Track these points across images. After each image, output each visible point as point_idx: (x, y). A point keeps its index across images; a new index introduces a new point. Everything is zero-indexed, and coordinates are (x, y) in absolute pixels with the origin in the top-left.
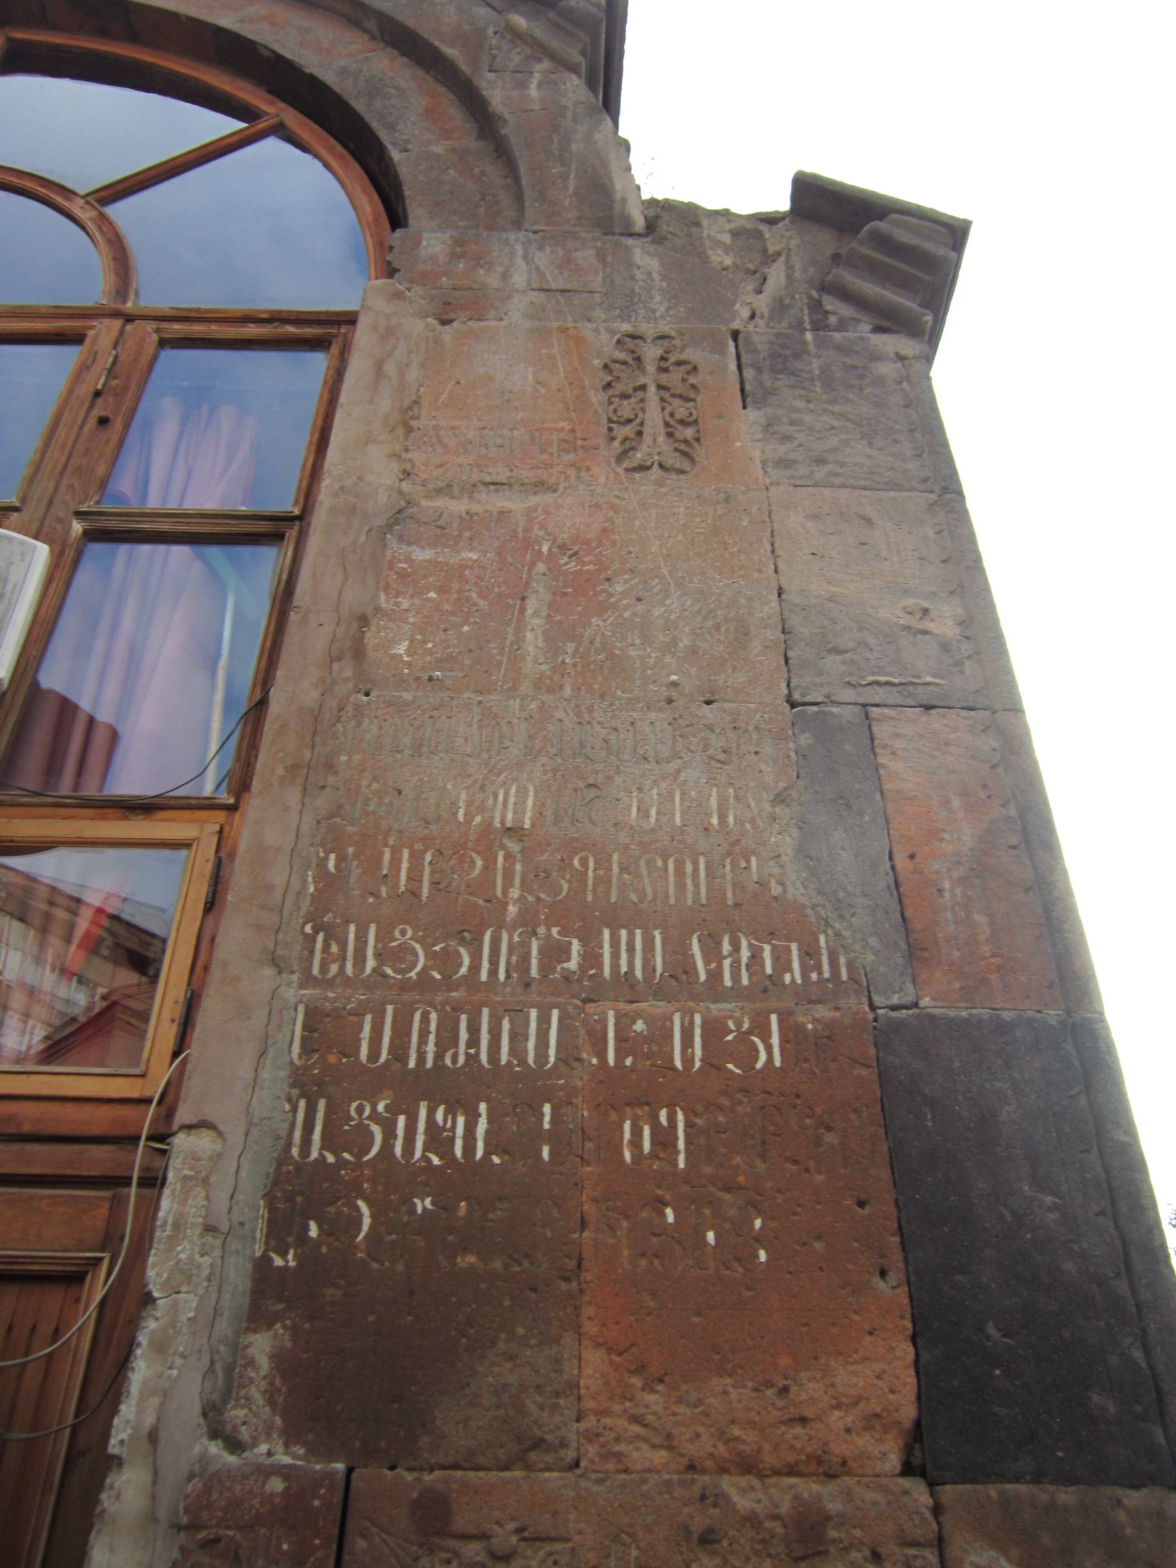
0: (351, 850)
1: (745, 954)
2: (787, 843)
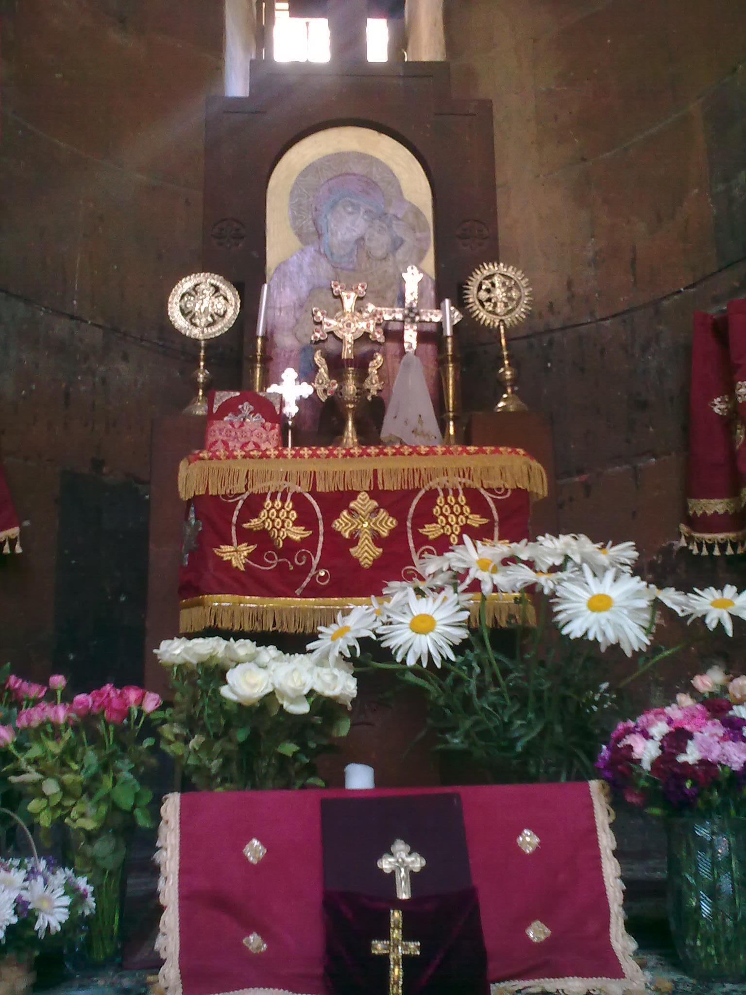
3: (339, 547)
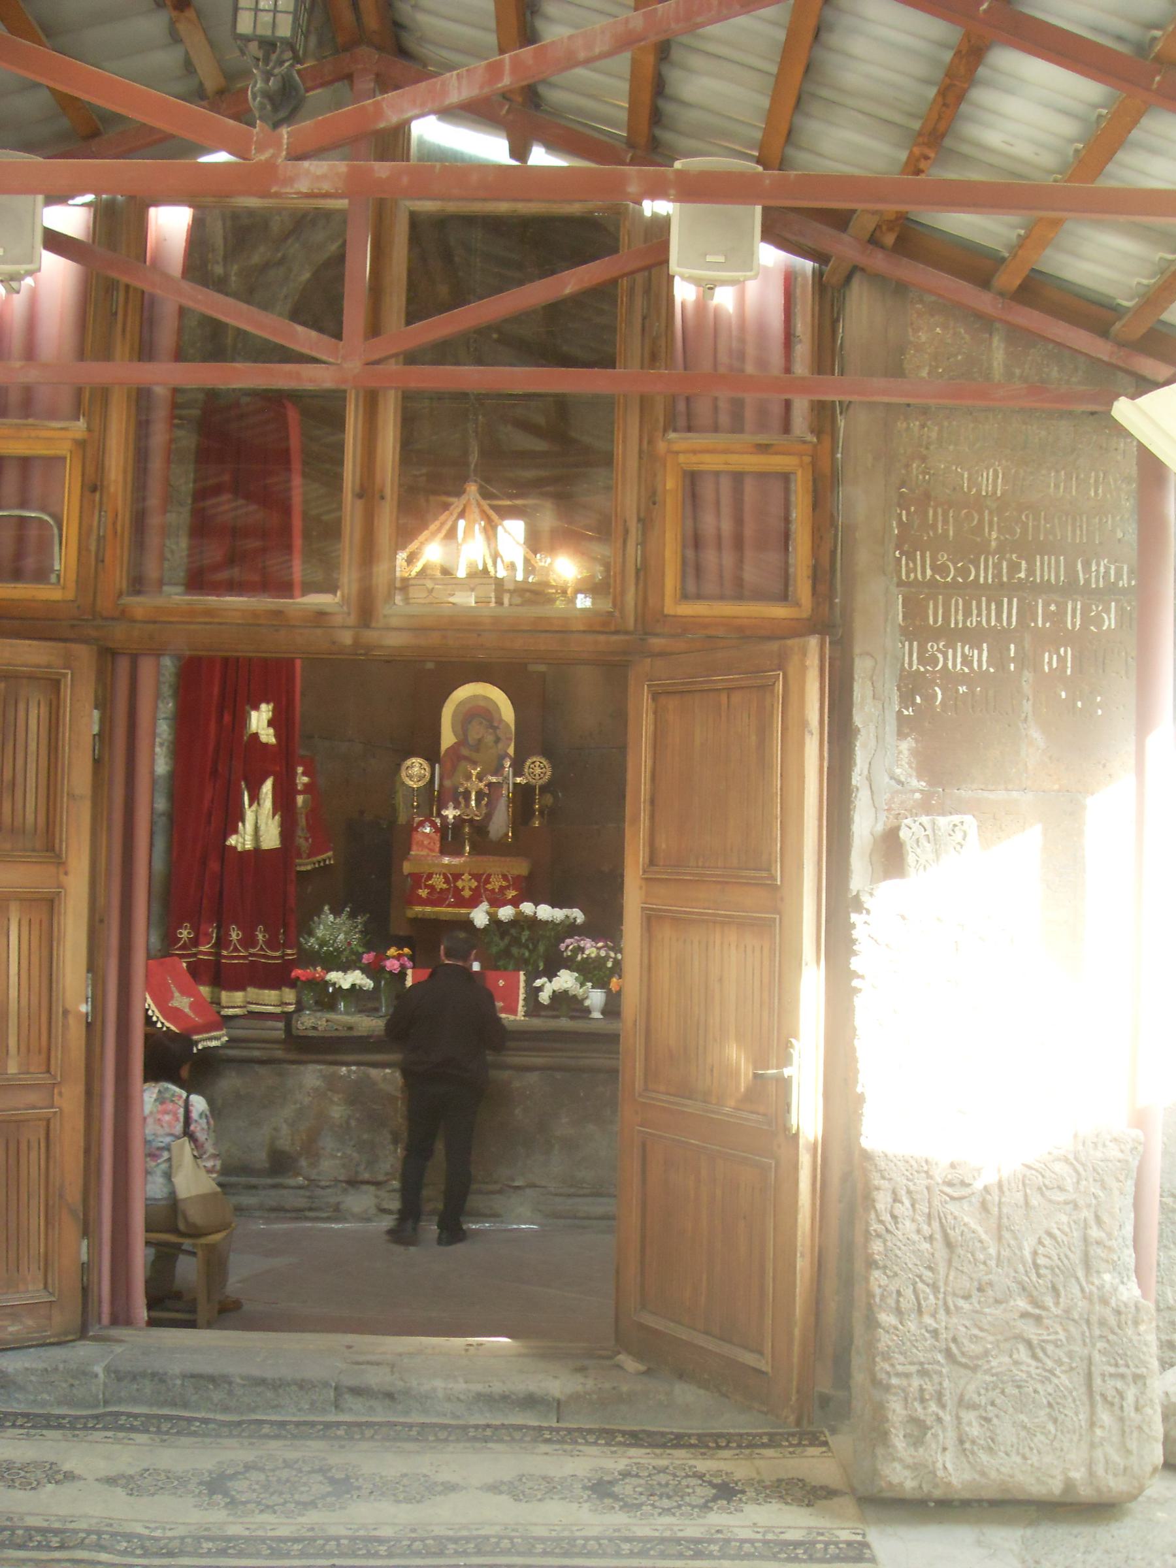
0: (913, 509)
1: (1102, 569)
3: (457, 892)
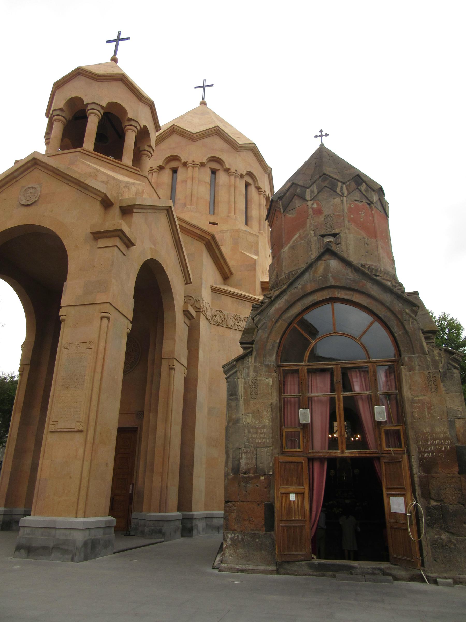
2: (448, 432)
